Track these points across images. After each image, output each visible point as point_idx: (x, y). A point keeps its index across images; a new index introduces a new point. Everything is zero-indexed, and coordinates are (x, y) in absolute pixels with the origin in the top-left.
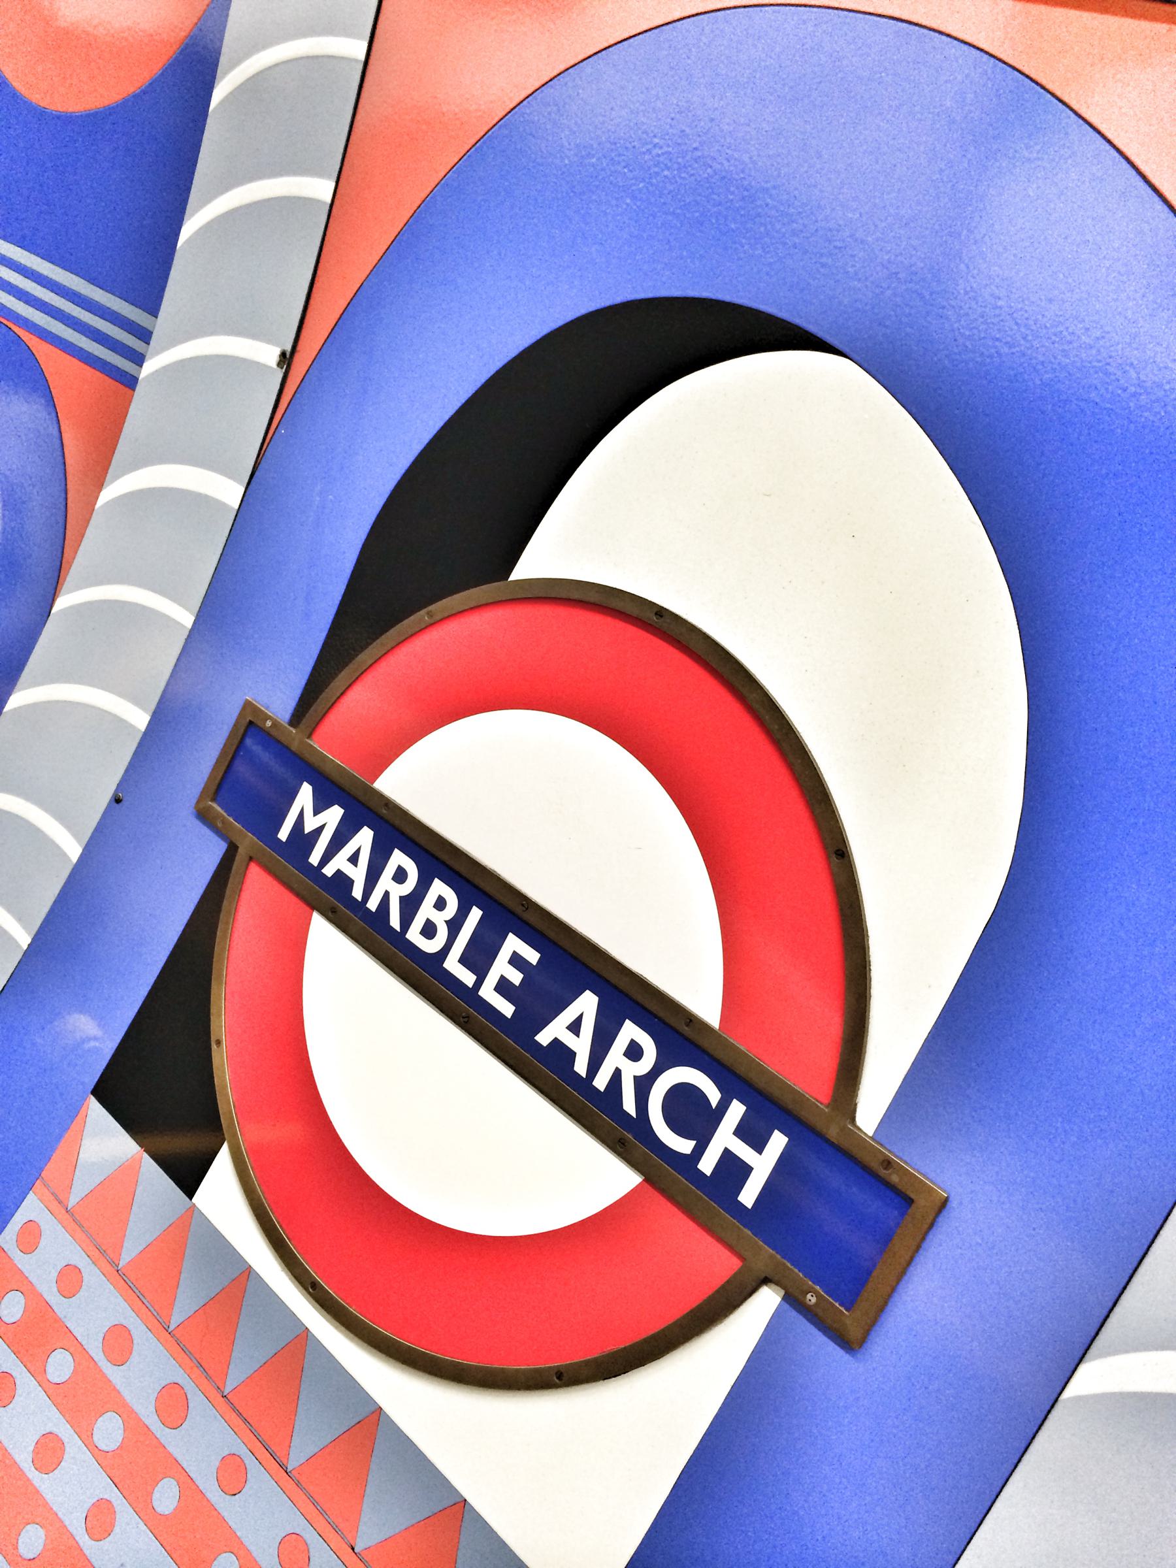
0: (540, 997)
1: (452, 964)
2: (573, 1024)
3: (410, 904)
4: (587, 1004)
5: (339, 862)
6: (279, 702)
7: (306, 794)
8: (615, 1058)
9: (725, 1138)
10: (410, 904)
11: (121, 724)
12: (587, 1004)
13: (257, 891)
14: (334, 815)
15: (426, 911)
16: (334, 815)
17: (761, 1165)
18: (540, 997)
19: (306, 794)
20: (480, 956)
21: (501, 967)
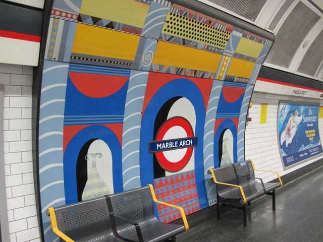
0: (178, 144)
1: (173, 147)
2: (181, 144)
3: (169, 146)
5: (163, 147)
6: (152, 141)
7: (158, 145)
9: (190, 142)
10: (169, 146)
11: (61, 135)
13: (157, 155)
14: (161, 144)
16: (161, 144)
18: (178, 144)
19: (158, 145)
20: (174, 145)
21: (176, 144)
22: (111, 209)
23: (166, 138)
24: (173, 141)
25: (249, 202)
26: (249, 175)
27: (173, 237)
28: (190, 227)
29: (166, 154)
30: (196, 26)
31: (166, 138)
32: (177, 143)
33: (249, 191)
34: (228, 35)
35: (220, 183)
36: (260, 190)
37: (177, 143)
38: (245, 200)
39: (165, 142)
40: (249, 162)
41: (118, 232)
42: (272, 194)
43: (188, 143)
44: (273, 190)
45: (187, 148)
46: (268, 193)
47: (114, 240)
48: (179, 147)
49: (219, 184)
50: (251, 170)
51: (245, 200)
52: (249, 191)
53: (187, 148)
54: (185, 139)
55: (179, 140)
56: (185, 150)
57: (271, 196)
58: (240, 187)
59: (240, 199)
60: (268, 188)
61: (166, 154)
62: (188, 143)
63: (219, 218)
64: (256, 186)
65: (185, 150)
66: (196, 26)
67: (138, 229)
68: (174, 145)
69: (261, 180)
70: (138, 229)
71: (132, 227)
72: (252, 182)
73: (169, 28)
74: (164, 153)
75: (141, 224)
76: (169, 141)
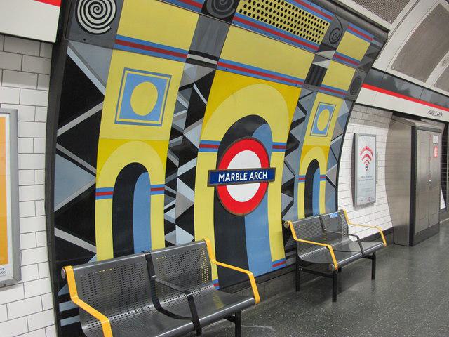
0: (248, 177)
1: (241, 179)
4: (252, 174)
6: (214, 167)
7: (220, 175)
8: (256, 176)
9: (264, 175)
12: (252, 174)
14: (224, 175)
15: (237, 177)
16: (224, 175)
17: (266, 175)
18: (248, 177)
19: (220, 175)
20: (242, 177)
21: (245, 176)
22: (151, 271)
23: (231, 167)
24: (242, 171)
25: (340, 269)
26: (341, 230)
27: (238, 312)
28: (262, 298)
29: (229, 187)
30: (279, 7)
31: (231, 167)
32: (246, 175)
33: (341, 252)
34: (324, 26)
35: (300, 240)
36: (356, 252)
37: (246, 175)
38: (336, 264)
39: (231, 172)
40: (343, 213)
41: (162, 303)
42: (372, 257)
43: (261, 175)
44: (374, 252)
45: (259, 184)
46: (367, 256)
47: (155, 316)
48: (249, 181)
49: (299, 242)
50: (343, 227)
51: (336, 264)
52: (341, 252)
53: (259, 184)
54: (258, 170)
55: (249, 171)
56: (257, 185)
57: (371, 260)
58: (330, 247)
59: (329, 264)
60: (369, 247)
61: (230, 188)
62: (261, 175)
63: (298, 289)
64: (350, 246)
65: (257, 185)
66: (278, 14)
67: (190, 298)
68: (242, 177)
69: (358, 238)
70: (190, 298)
71: (184, 296)
72: (344, 241)
73: (247, 9)
74: (229, 187)
75: (193, 293)
76: (235, 171)
